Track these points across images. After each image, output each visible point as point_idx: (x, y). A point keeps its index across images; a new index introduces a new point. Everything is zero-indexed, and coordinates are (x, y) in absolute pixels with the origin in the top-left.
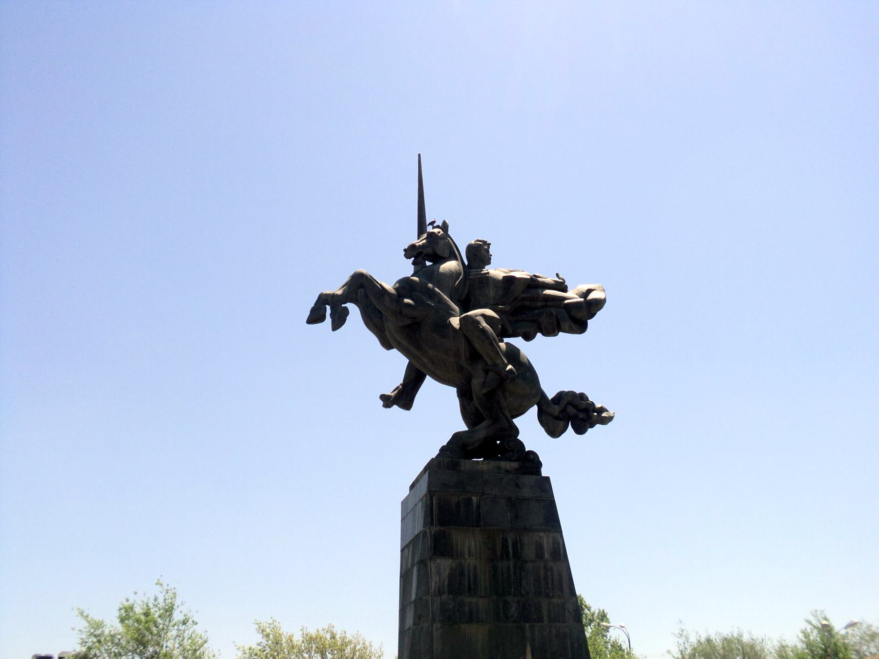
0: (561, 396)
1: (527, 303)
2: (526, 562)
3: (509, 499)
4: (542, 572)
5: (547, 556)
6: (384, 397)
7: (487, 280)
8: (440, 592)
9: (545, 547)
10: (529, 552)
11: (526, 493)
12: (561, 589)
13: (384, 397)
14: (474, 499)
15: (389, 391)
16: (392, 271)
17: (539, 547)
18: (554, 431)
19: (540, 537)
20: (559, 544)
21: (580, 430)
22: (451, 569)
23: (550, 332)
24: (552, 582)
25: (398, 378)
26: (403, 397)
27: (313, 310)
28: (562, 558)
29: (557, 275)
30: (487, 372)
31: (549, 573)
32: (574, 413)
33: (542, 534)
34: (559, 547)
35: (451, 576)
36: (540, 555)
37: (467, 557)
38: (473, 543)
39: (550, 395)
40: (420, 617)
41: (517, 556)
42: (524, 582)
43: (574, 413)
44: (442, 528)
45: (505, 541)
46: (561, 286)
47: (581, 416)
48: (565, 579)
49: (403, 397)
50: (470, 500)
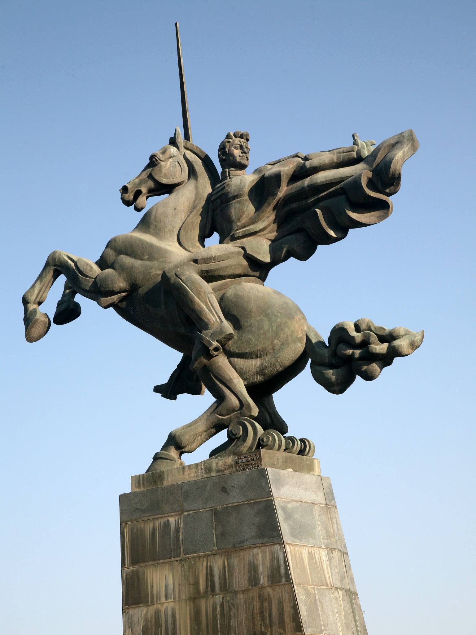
1: (294, 205)
2: (236, 593)
3: (216, 513)
4: (257, 605)
5: (263, 580)
6: (157, 389)
9: (261, 569)
10: (240, 580)
12: (282, 623)
13: (157, 389)
14: (172, 520)
15: (164, 379)
17: (253, 569)
19: (253, 555)
20: (278, 561)
22: (146, 620)
24: (270, 616)
28: (283, 580)
31: (266, 604)
33: (255, 551)
34: (279, 568)
36: (254, 580)
37: (163, 600)
38: (171, 581)
41: (225, 588)
42: (233, 623)
44: (135, 568)
48: (287, 609)
50: (167, 524)
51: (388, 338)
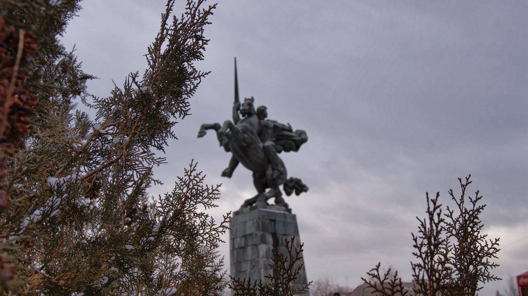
0: (292, 180)
7: (267, 127)
8: (263, 258)
11: (289, 220)
16: (224, 115)
18: (289, 194)
21: (298, 194)
23: (287, 150)
25: (226, 165)
26: (228, 173)
27: (200, 133)
29: (288, 124)
30: (273, 169)
32: (297, 187)
35: (266, 252)
39: (288, 177)
40: (254, 267)
43: (297, 187)
45: (282, 240)
46: (290, 130)
47: (300, 188)
49: (228, 173)
51: (305, 186)
